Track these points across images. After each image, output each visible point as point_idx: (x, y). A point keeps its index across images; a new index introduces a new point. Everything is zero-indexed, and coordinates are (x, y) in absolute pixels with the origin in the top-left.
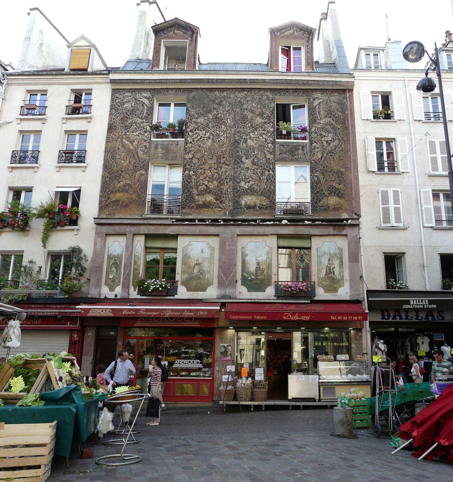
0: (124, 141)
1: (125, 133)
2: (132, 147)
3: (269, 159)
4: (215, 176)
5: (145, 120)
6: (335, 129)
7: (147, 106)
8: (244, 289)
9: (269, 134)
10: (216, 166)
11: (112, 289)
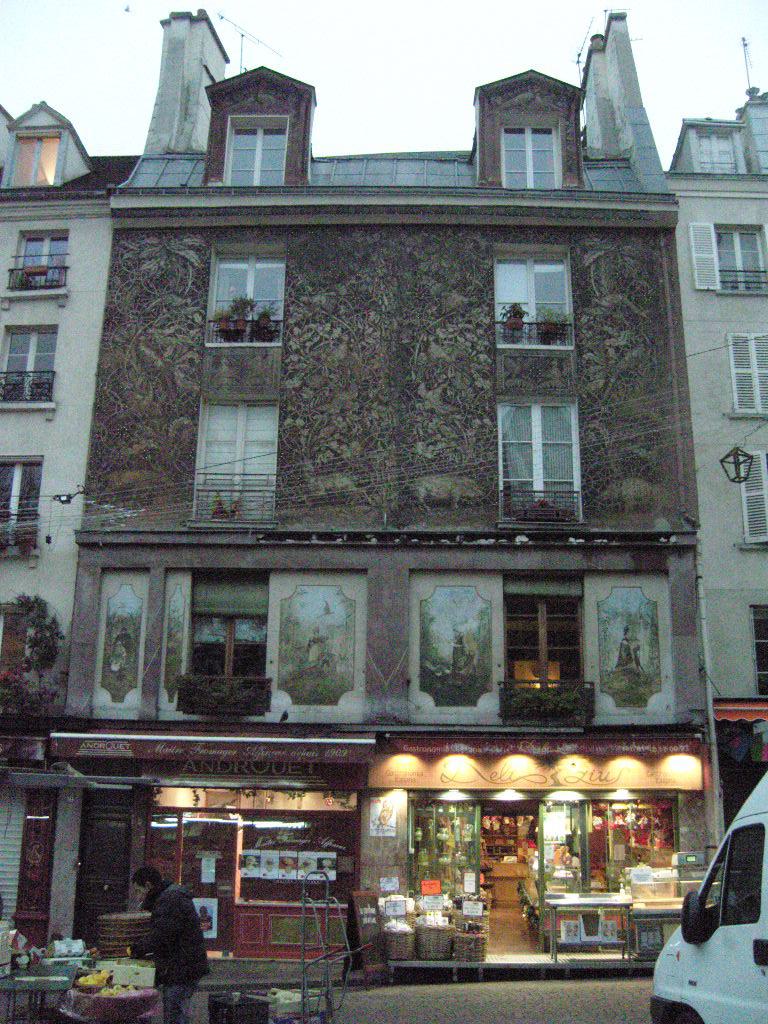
0: (143, 348)
1: (145, 330)
2: (160, 363)
3: (482, 389)
4: (355, 431)
5: (189, 300)
6: (634, 319)
7: (194, 267)
8: (426, 701)
9: (480, 331)
10: (356, 409)
11: (118, 697)
